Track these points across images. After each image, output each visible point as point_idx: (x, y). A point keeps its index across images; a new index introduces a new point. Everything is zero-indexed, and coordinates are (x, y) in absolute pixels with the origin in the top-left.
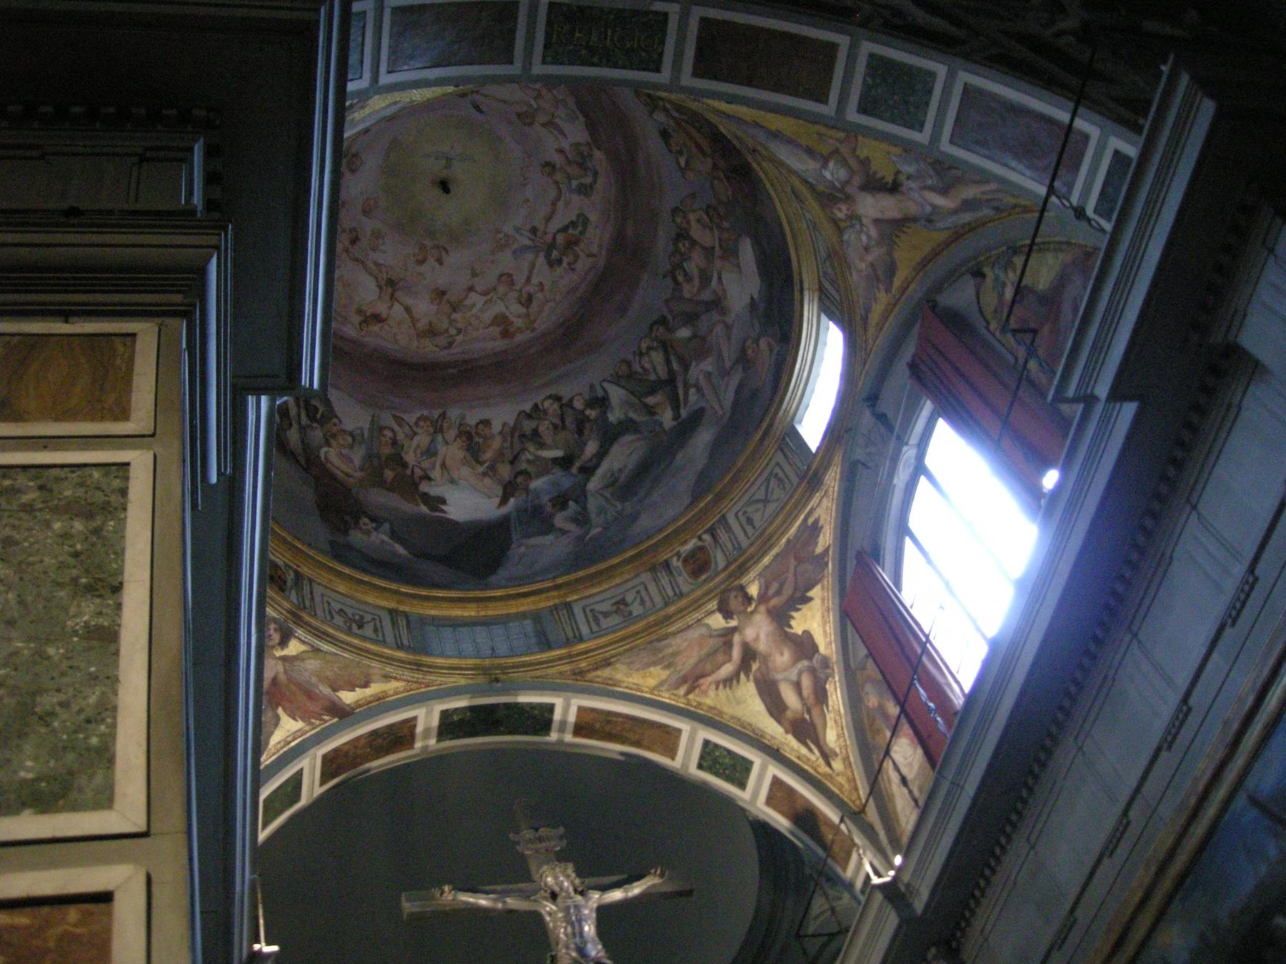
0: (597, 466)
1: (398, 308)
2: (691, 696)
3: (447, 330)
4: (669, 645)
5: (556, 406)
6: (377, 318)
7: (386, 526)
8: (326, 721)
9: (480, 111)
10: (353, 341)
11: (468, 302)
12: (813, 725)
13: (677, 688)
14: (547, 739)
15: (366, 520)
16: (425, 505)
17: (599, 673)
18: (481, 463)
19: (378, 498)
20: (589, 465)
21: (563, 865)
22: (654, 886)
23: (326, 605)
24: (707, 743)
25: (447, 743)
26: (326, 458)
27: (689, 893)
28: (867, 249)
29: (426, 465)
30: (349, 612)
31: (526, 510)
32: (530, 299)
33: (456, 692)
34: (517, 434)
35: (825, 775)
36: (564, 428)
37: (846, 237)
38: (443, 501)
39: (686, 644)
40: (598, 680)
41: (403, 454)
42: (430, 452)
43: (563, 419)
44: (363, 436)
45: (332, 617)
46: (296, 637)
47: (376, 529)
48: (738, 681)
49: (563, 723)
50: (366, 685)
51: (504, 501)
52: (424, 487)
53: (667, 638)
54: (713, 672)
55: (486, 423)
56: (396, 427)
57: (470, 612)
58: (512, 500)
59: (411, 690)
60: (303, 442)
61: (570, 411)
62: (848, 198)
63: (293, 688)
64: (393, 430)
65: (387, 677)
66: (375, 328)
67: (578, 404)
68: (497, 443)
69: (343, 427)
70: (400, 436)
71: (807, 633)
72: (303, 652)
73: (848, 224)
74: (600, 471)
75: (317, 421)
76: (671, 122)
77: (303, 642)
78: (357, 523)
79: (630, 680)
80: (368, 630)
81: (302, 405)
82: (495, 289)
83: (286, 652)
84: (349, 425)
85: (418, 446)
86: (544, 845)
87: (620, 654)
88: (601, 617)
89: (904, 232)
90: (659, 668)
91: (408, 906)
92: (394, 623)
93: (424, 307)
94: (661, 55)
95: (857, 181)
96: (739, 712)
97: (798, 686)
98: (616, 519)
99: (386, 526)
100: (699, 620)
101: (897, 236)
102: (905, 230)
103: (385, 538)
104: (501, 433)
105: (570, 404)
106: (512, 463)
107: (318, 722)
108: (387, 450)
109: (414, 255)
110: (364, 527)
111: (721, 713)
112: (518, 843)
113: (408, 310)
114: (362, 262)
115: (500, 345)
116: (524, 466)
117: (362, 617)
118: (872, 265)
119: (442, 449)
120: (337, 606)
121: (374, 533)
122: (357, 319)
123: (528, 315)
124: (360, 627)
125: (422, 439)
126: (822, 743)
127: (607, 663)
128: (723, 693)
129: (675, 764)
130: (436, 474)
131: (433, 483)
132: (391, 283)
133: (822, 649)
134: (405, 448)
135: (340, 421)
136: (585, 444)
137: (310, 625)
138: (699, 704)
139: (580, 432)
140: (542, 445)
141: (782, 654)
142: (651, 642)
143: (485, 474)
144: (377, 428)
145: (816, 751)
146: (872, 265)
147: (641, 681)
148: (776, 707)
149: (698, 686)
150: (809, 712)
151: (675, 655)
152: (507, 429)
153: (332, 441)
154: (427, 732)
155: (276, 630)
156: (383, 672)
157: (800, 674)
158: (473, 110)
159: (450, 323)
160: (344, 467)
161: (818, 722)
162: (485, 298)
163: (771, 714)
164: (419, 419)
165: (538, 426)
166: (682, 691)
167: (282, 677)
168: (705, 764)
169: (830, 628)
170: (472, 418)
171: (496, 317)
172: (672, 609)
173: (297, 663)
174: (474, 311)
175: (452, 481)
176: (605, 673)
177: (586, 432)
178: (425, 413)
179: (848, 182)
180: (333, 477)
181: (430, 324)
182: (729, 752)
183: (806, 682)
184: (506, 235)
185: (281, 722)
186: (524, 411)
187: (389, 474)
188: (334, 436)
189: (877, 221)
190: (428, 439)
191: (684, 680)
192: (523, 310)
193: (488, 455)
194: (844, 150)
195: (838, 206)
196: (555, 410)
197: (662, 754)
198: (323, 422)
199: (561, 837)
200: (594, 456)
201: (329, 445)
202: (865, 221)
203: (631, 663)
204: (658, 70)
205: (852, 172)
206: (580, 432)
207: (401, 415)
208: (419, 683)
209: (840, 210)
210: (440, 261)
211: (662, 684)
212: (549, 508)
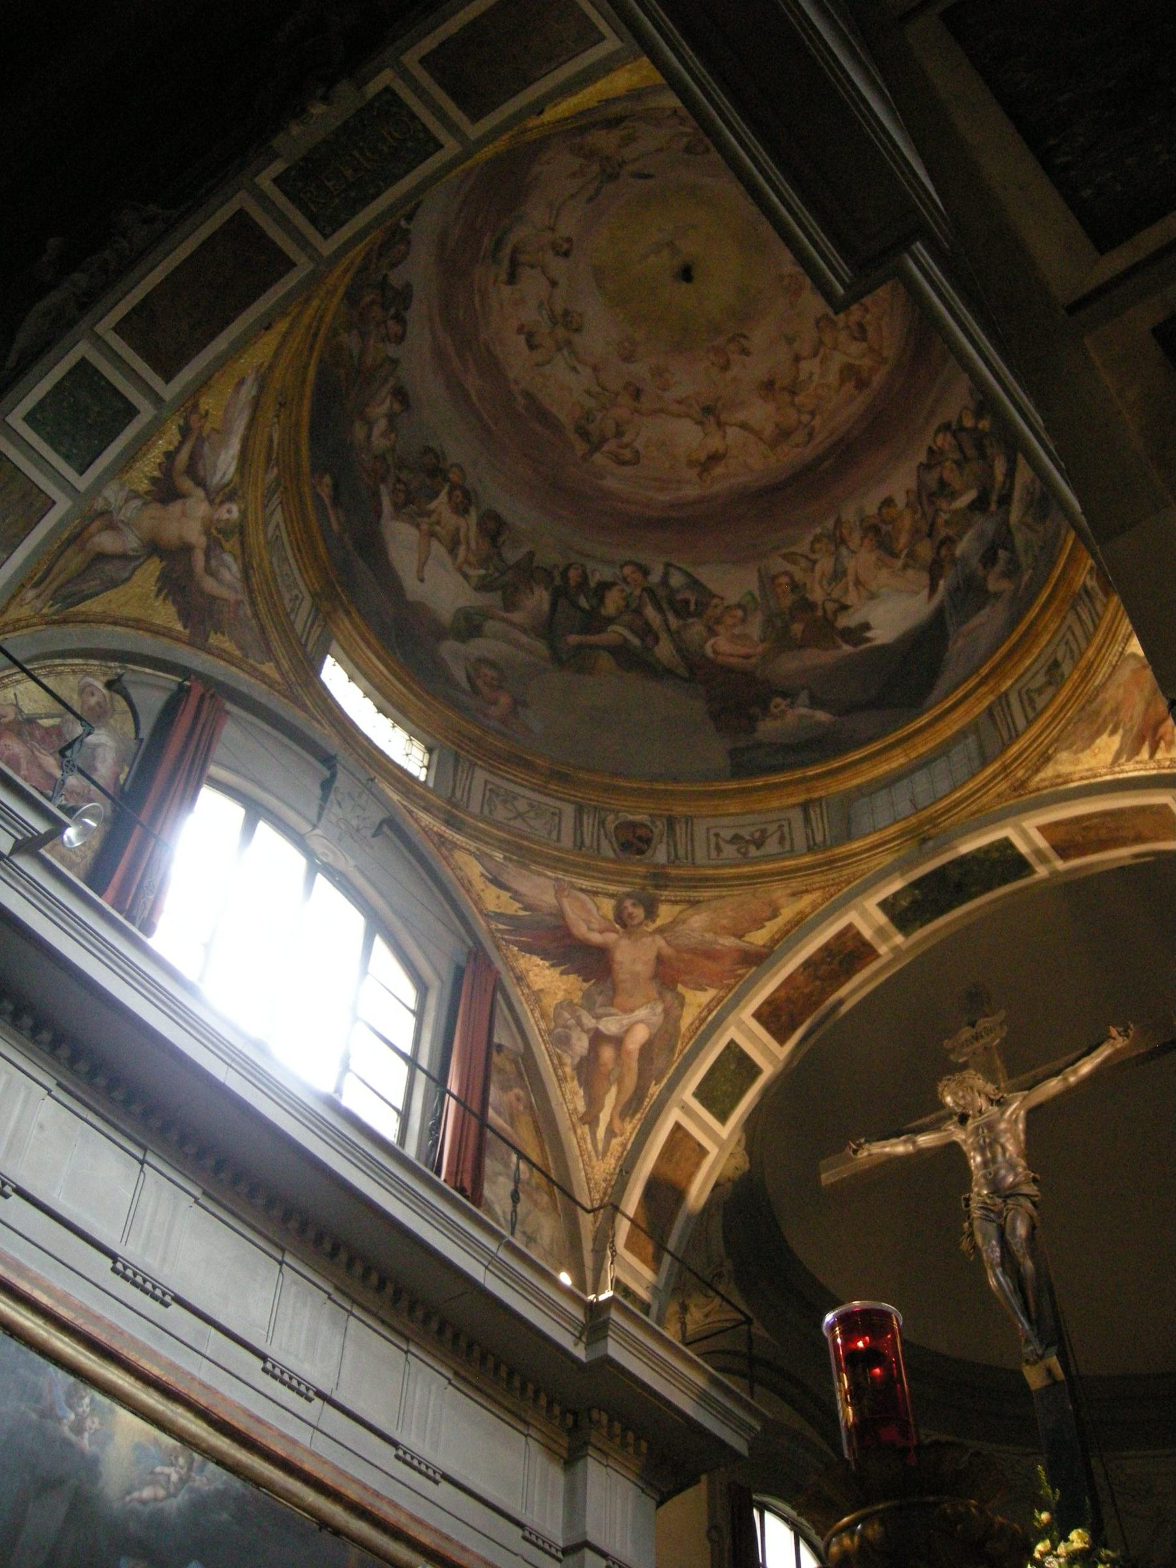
0: (1012, 488)
1: (733, 433)
2: (1159, 755)
3: (800, 423)
4: (1105, 702)
5: (949, 437)
6: (715, 458)
7: (804, 696)
8: (742, 976)
9: (648, 176)
10: (701, 500)
11: (803, 376)
14: (1036, 877)
15: (778, 700)
16: (847, 642)
17: (1041, 775)
18: (895, 555)
19: (791, 664)
20: (1004, 492)
22: (1117, 1052)
23: (713, 839)
25: (919, 934)
26: (715, 652)
29: (835, 594)
30: (745, 833)
31: (958, 588)
32: (861, 326)
33: (883, 875)
34: (925, 502)
36: (966, 459)
38: (866, 627)
39: (1121, 691)
40: (1046, 783)
41: (808, 596)
42: (838, 575)
43: (961, 449)
44: (754, 598)
45: (719, 849)
46: (662, 901)
47: (792, 705)
49: (1038, 852)
50: (775, 914)
51: (933, 588)
52: (844, 621)
53: (1097, 695)
55: (888, 502)
56: (790, 567)
57: (897, 761)
58: (942, 583)
59: (832, 896)
60: (679, 650)
61: (964, 434)
63: (687, 956)
64: (786, 573)
65: (796, 894)
66: (719, 470)
67: (969, 423)
68: (907, 523)
69: (726, 603)
70: (799, 576)
72: (681, 912)
74: (1017, 494)
75: (690, 615)
77: (675, 902)
78: (765, 709)
79: (1080, 767)
80: (772, 846)
81: (665, 606)
82: (821, 342)
83: (659, 922)
84: (733, 596)
85: (823, 575)
86: (982, 1041)
87: (1056, 740)
88: (1035, 696)
90: (1105, 737)
92: (807, 820)
93: (760, 413)
94: (425, 129)
98: (1042, 548)
99: (804, 696)
100: (1122, 653)
103: (803, 711)
104: (907, 505)
105: (962, 429)
106: (930, 535)
107: (732, 981)
108: (788, 601)
109: (713, 364)
110: (774, 710)
113: (744, 426)
114: (661, 411)
115: (863, 399)
116: (943, 532)
117: (763, 831)
119: (850, 564)
120: (727, 834)
121: (791, 711)
122: (692, 474)
123: (871, 349)
124: (759, 844)
125: (825, 564)
127: (1046, 759)
130: (851, 598)
131: (851, 611)
132: (708, 410)
134: (809, 585)
135: (722, 598)
136: (991, 467)
137: (680, 879)
139: (983, 455)
140: (954, 496)
142: (1083, 708)
143: (905, 567)
144: (768, 581)
147: (1093, 763)
149: (1161, 738)
151: (1115, 711)
152: (912, 498)
153: (716, 627)
154: (880, 932)
155: (634, 905)
156: (789, 891)
158: (641, 181)
159: (799, 411)
160: (744, 651)
162: (818, 359)
164: (812, 543)
165: (941, 472)
167: (668, 951)
170: (871, 508)
171: (841, 372)
172: (1090, 653)
173: (680, 928)
174: (816, 377)
175: (873, 596)
176: (1048, 772)
177: (989, 451)
178: (818, 530)
180: (729, 670)
181: (777, 425)
184: (791, 276)
185: (687, 1000)
186: (921, 464)
187: (797, 628)
188: (718, 621)
190: (832, 560)
192: (864, 345)
193: (903, 540)
196: (950, 444)
198: (701, 609)
200: (1006, 475)
201: (712, 632)
203: (1072, 745)
204: (441, 146)
206: (983, 455)
207: (792, 549)
208: (838, 884)
210: (745, 352)
212: (981, 572)
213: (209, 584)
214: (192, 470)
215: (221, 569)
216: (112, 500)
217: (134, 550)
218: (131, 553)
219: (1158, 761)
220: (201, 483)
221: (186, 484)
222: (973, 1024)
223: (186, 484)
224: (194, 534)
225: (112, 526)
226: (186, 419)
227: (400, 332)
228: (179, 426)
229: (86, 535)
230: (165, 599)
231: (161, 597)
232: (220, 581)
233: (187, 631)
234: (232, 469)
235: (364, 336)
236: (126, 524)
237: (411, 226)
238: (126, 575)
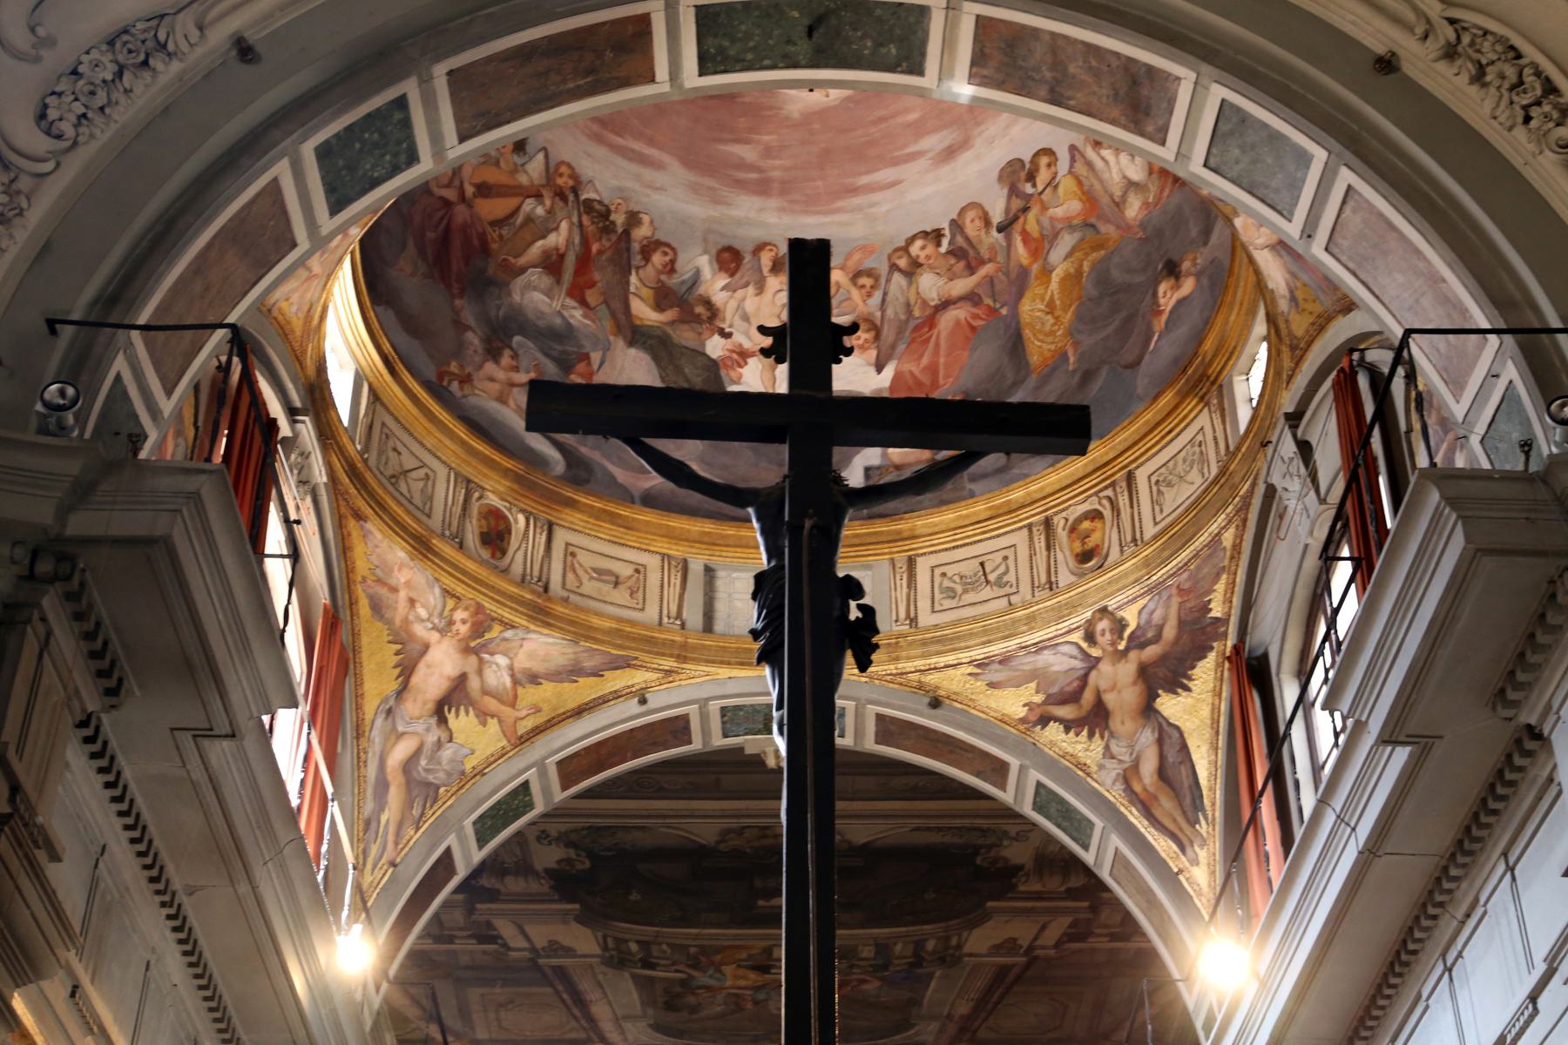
28: (412, 602)
37: (437, 591)
62: (467, 650)
73: (446, 613)
76: (523, 179)
89: (396, 667)
95: (474, 684)
101: (397, 653)
102: (398, 670)
118: (394, 590)
146: (394, 590)
179: (480, 672)
189: (426, 647)
194: (507, 711)
195: (468, 625)
202: (435, 636)
205: (485, 692)
209: (464, 622)
213: (1170, 632)
214: (1073, 697)
215: (1154, 623)
216: (1114, 774)
217: (1153, 732)
218: (1156, 735)
220: (1084, 679)
221: (1088, 697)
223: (1088, 697)
224: (1128, 669)
225: (1136, 765)
226: (1035, 725)
227: (1044, 161)
228: (1043, 728)
229: (1143, 796)
230: (1190, 679)
231: (1190, 684)
232: (1165, 619)
233: (1215, 644)
234: (1066, 649)
235: (1056, 235)
236: (1132, 747)
237: (945, 225)
238: (1176, 735)
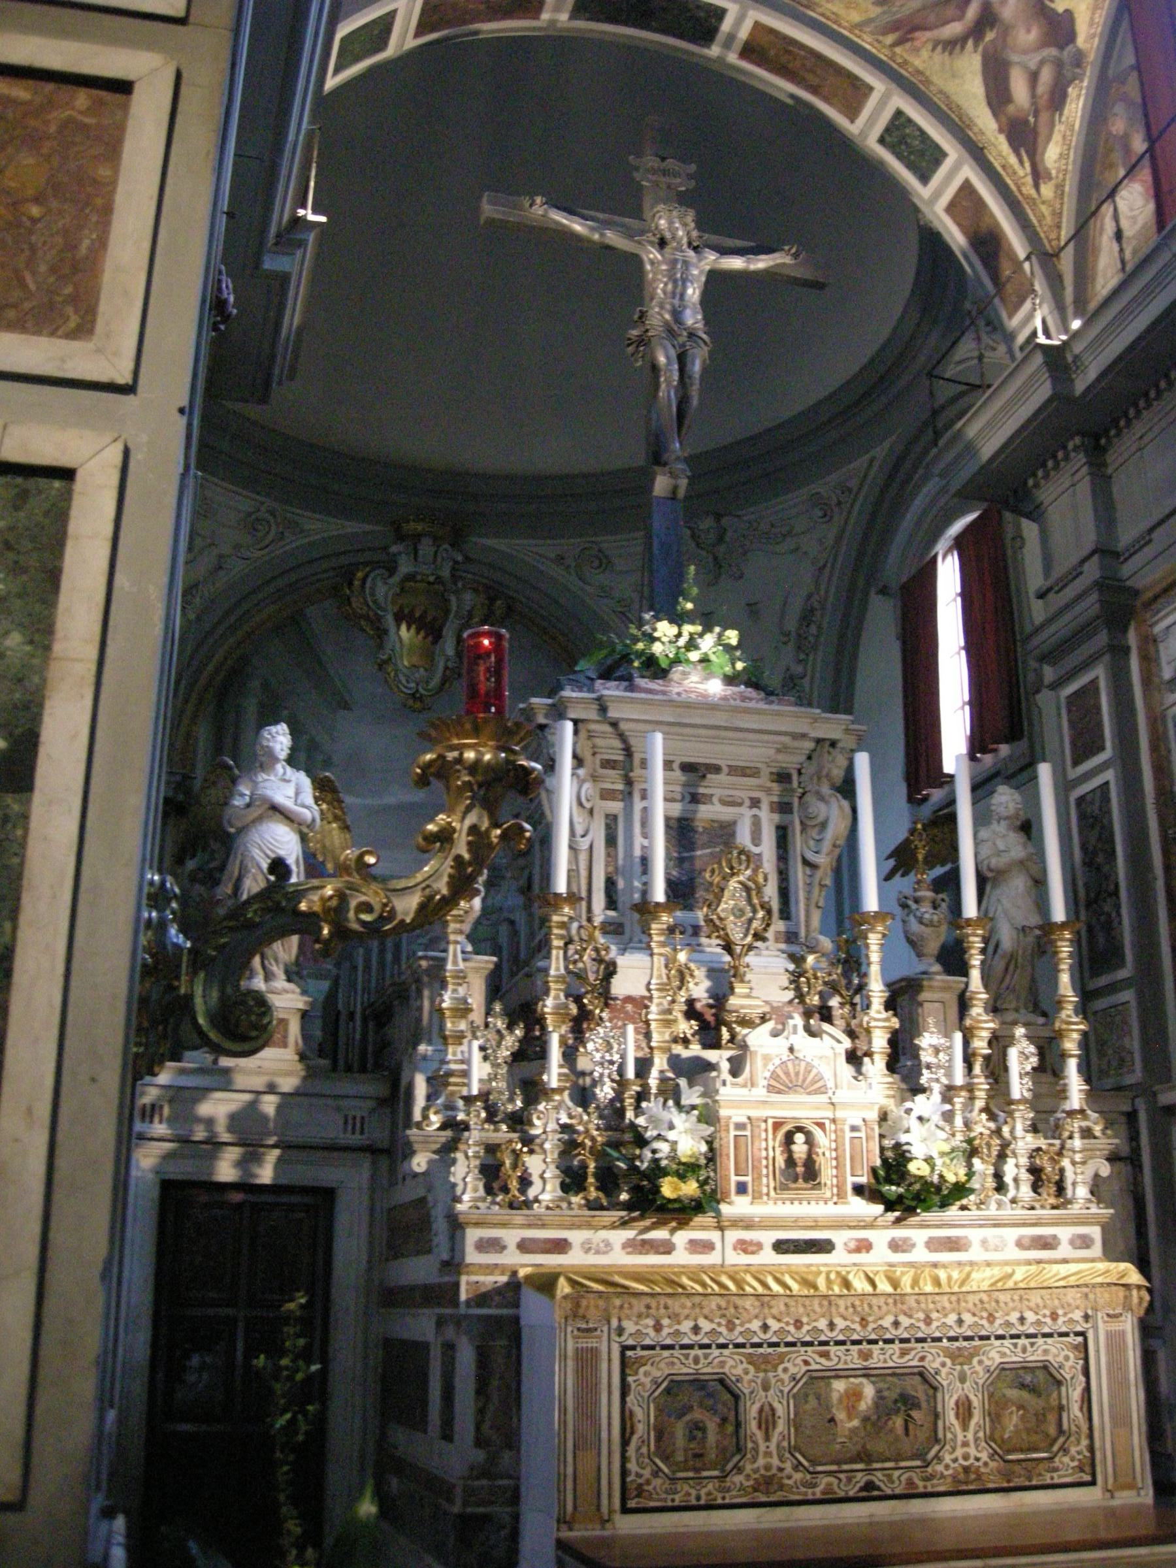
2: (898, 50)
12: (1035, 132)
13: (884, 34)
14: (706, 51)
21: (683, 209)
22: (784, 264)
24: (899, 113)
25: (581, 24)
27: (818, 286)
35: (1028, 198)
48: (963, 48)
49: (731, 37)
54: (937, 27)
71: (1069, 13)
86: (667, 180)
91: (488, 209)
96: (951, 88)
97: (1034, 77)
111: (928, 82)
112: (637, 169)
126: (1038, 158)
128: (939, 57)
129: (853, 128)
133: (1081, 41)
138: (906, 62)
141: (1029, 31)
145: (1027, 165)
147: (842, 12)
148: (998, 96)
149: (912, 39)
150: (1036, 115)
157: (1042, 63)
161: (1043, 130)
163: (990, 104)
166: (889, 39)
168: (888, 139)
169: (1101, 17)
182: (922, 133)
183: (1046, 76)
191: (894, 27)
197: (840, 112)
199: (690, 177)
211: (869, 21)
219: (894, 54)
222: (663, 159)
